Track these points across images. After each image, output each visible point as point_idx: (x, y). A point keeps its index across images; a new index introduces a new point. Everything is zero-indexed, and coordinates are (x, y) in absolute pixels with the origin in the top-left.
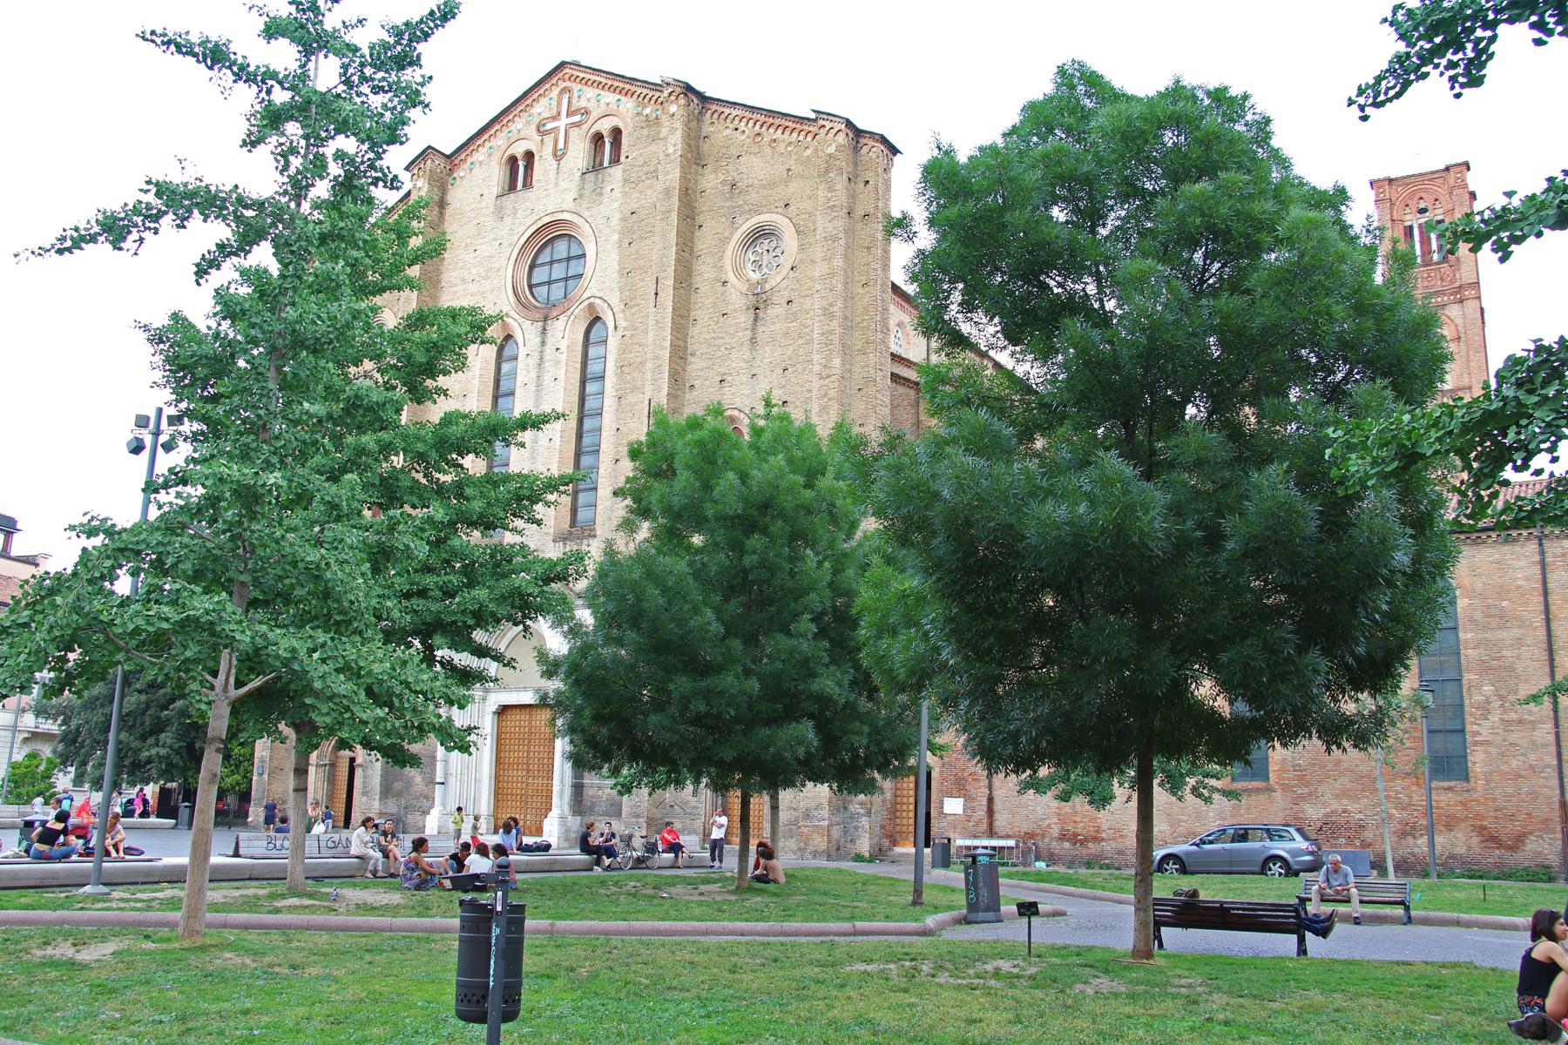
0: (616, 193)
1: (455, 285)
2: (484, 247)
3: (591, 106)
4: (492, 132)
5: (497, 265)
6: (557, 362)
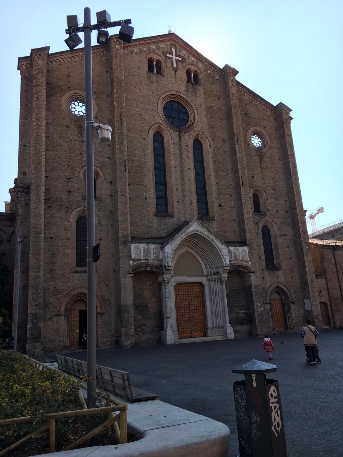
0: (202, 96)
1: (131, 100)
3: (186, 57)
4: (141, 43)
6: (188, 151)
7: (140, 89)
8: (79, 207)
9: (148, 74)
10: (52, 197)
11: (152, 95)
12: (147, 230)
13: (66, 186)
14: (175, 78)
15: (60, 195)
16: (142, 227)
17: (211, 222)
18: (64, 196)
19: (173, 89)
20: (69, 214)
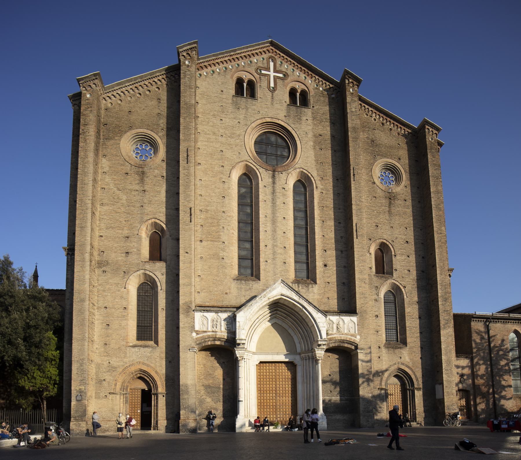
0: (310, 122)
2: (228, 120)
3: (289, 72)
5: (238, 133)
7: (222, 119)
8: (138, 271)
9: (234, 99)
10: (107, 260)
11: (238, 125)
12: (223, 297)
13: (123, 247)
14: (272, 101)
15: (116, 258)
16: (216, 293)
17: (310, 286)
18: (120, 259)
19: (268, 115)
20: (125, 280)
